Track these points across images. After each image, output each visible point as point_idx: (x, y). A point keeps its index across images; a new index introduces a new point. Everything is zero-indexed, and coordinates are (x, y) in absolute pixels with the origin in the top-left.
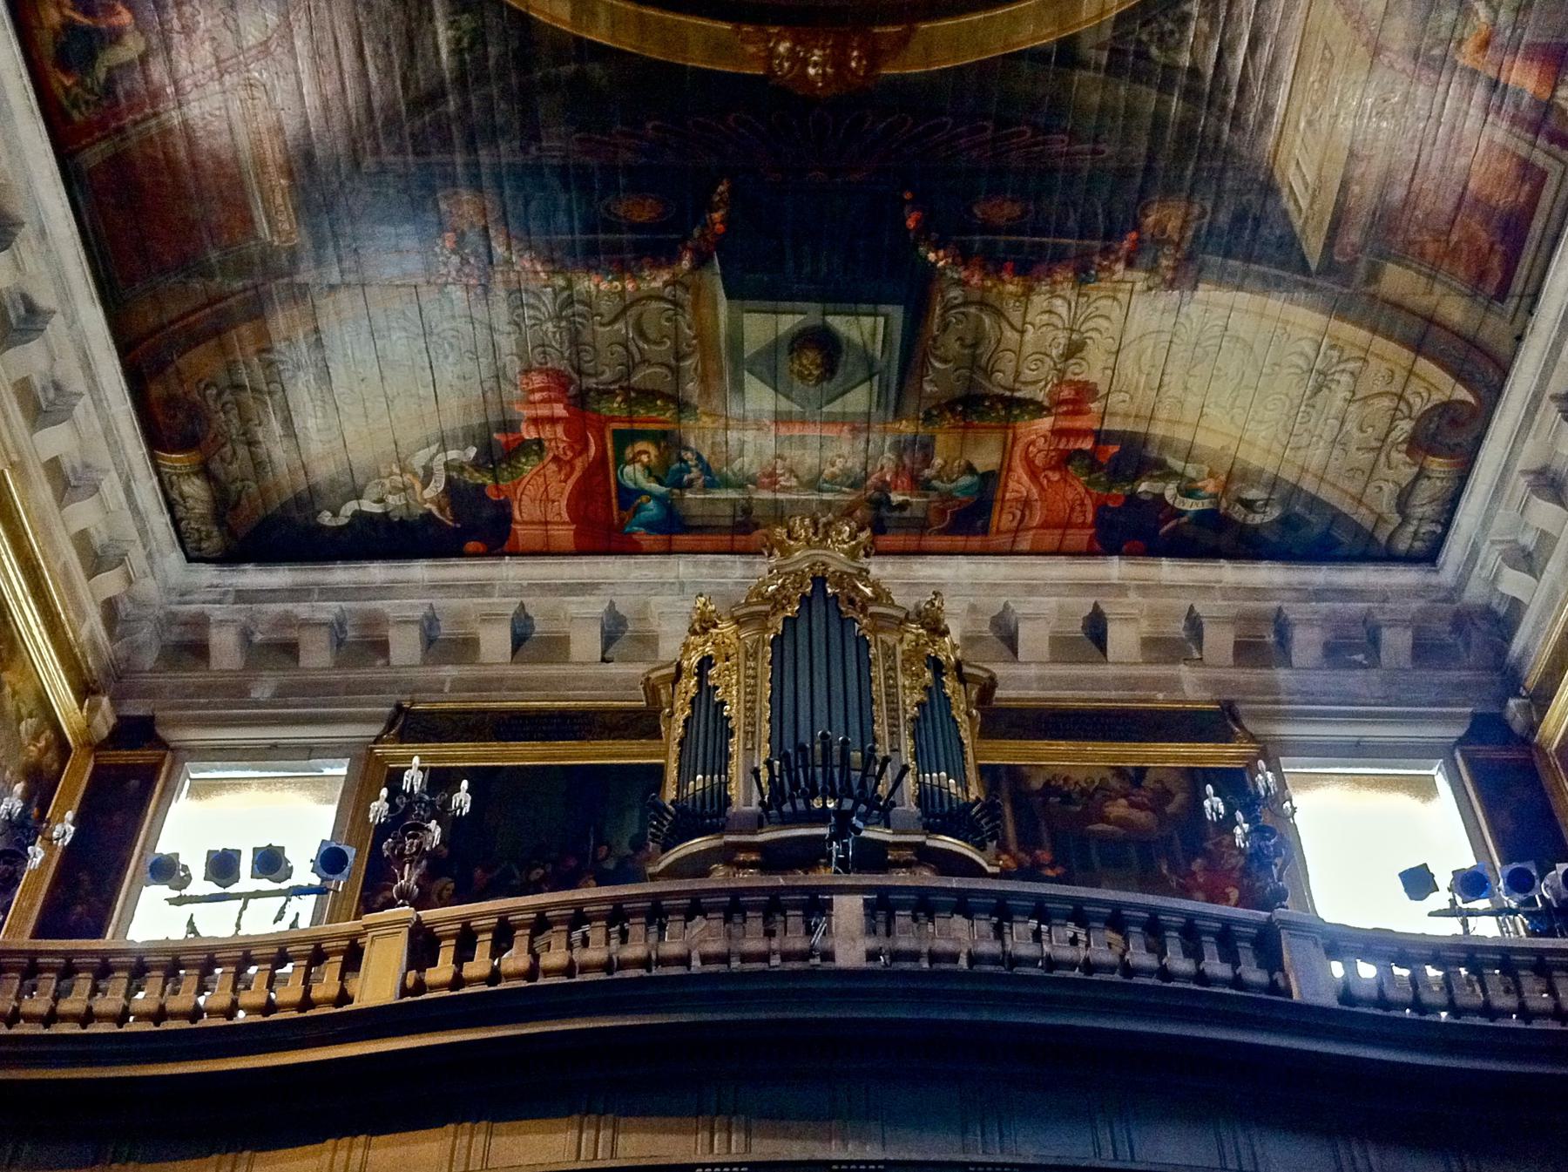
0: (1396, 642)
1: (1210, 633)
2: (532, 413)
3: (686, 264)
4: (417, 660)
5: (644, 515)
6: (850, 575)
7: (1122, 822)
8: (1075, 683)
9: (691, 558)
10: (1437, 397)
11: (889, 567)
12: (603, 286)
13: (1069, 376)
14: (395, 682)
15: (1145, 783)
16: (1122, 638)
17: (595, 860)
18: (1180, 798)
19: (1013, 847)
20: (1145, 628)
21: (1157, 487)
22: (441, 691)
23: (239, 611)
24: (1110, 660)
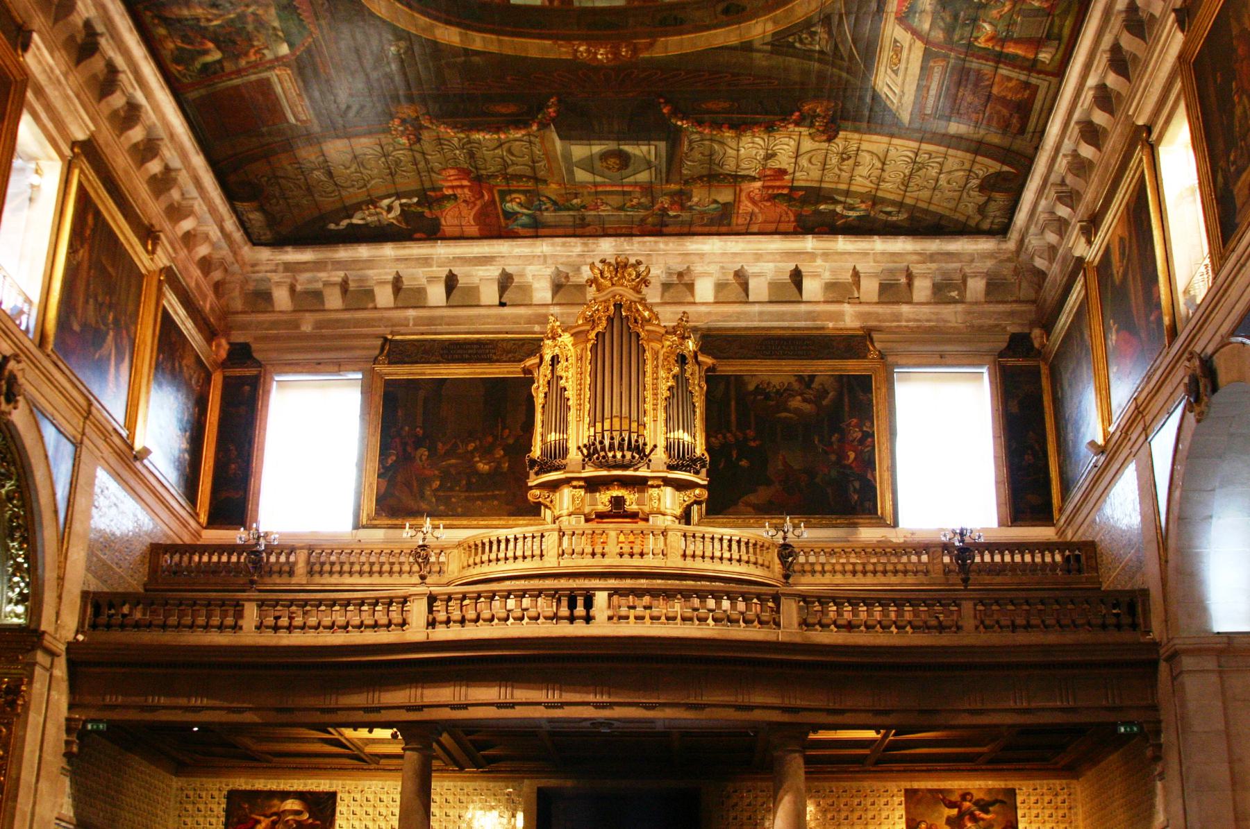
0: (976, 287)
1: (864, 283)
2: (450, 184)
3: (535, 128)
4: (392, 305)
5: (519, 222)
6: (635, 302)
7: (797, 411)
8: (781, 316)
9: (549, 240)
10: (991, 171)
11: (671, 244)
12: (487, 137)
13: (769, 166)
14: (380, 319)
15: (813, 386)
16: (812, 287)
17: (502, 438)
18: (831, 394)
19: (734, 429)
20: (827, 276)
21: (831, 207)
22: (407, 326)
23: (287, 277)
24: (805, 297)
